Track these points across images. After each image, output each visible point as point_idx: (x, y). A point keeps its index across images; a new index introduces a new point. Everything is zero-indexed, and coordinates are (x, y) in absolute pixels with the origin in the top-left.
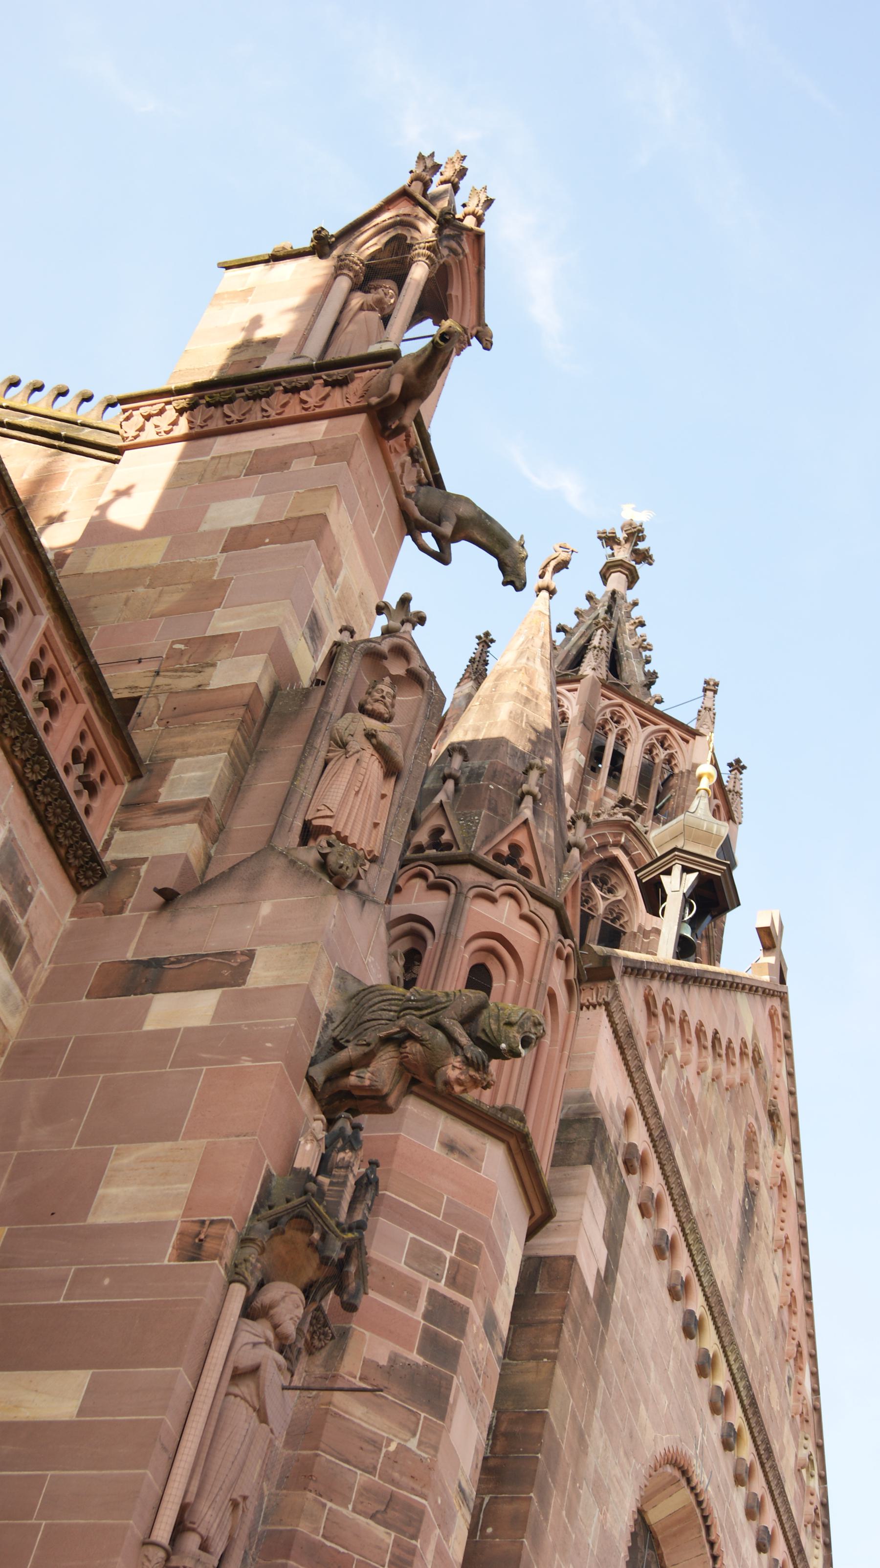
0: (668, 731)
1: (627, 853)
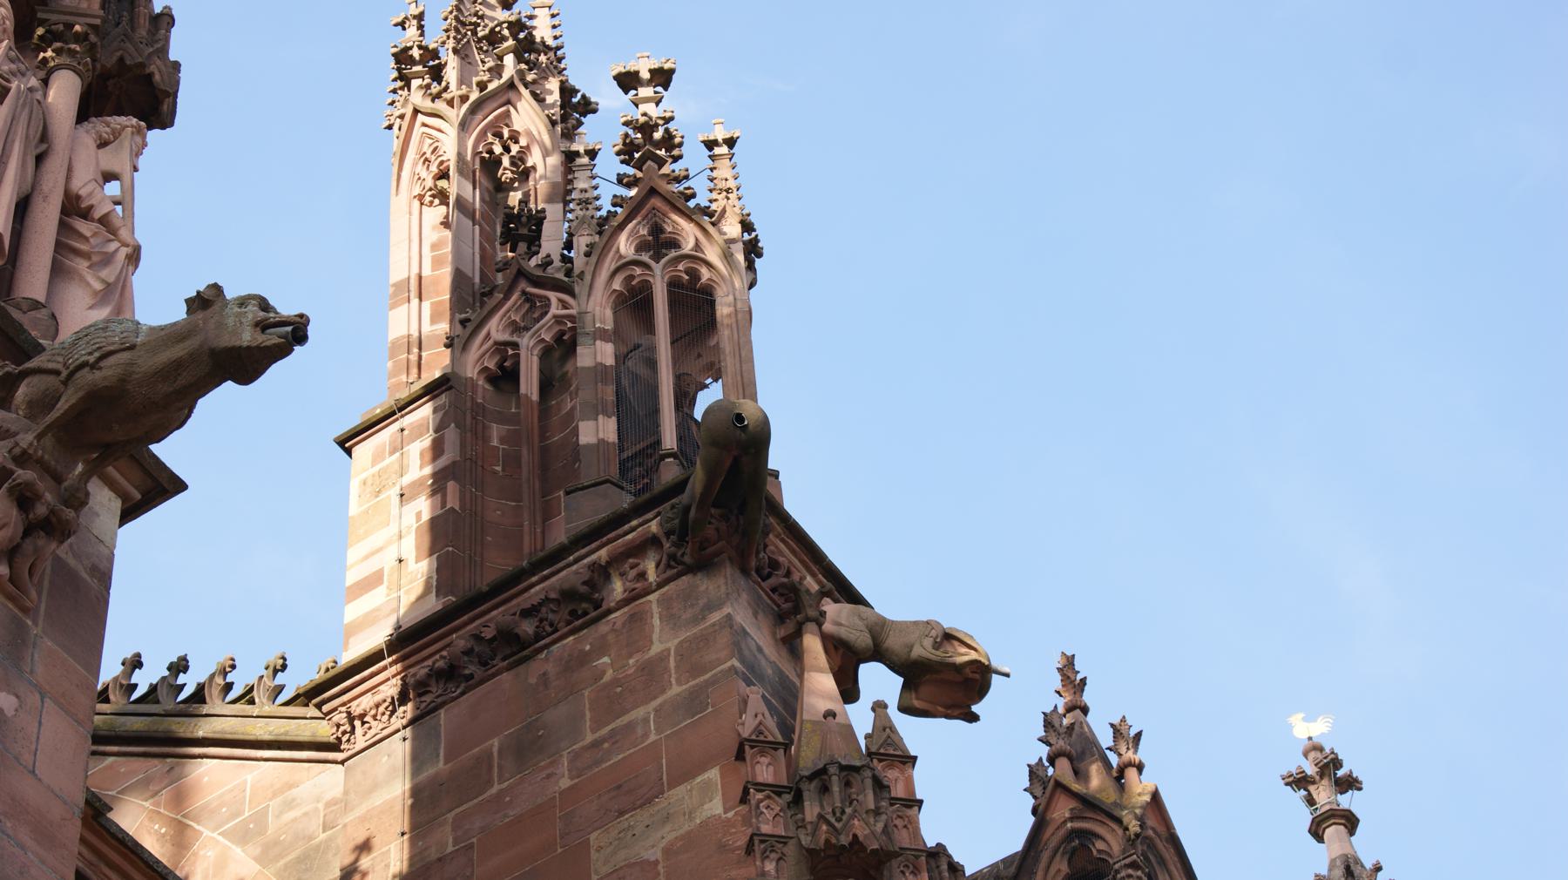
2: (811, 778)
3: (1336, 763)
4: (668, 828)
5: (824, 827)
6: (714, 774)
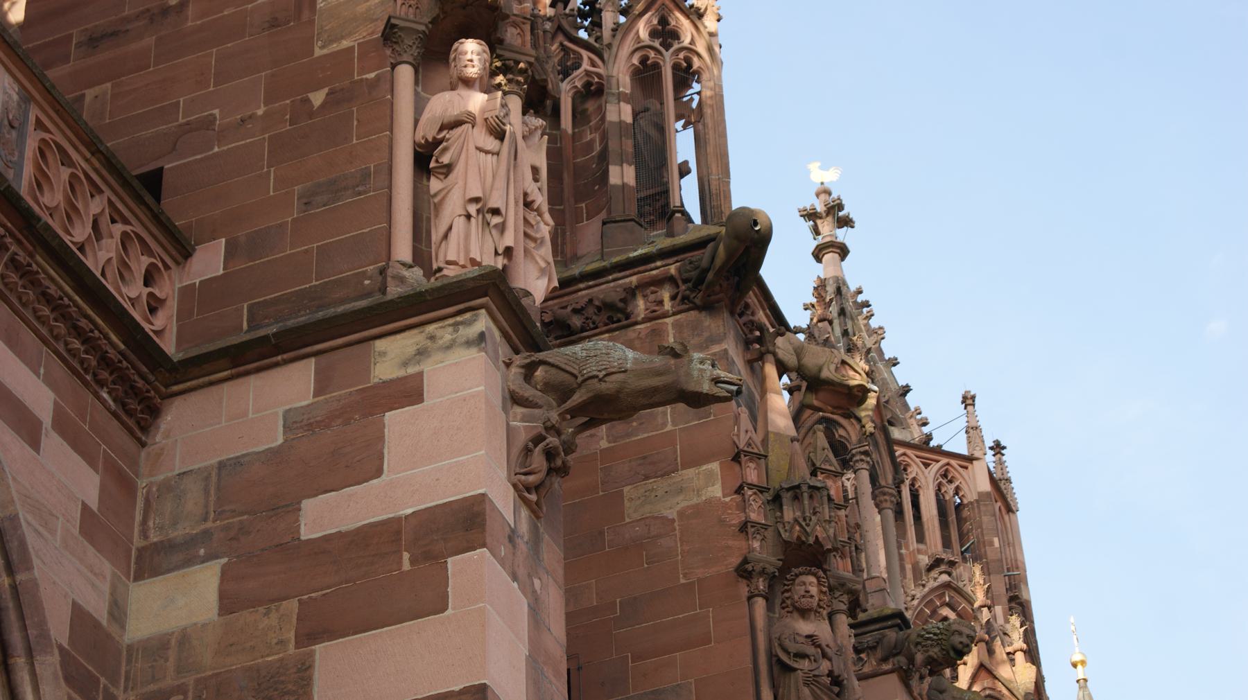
0: (948, 464)
1: (953, 609)
2: (788, 490)
3: (840, 207)
4: (681, 497)
5: (797, 528)
6: (715, 466)
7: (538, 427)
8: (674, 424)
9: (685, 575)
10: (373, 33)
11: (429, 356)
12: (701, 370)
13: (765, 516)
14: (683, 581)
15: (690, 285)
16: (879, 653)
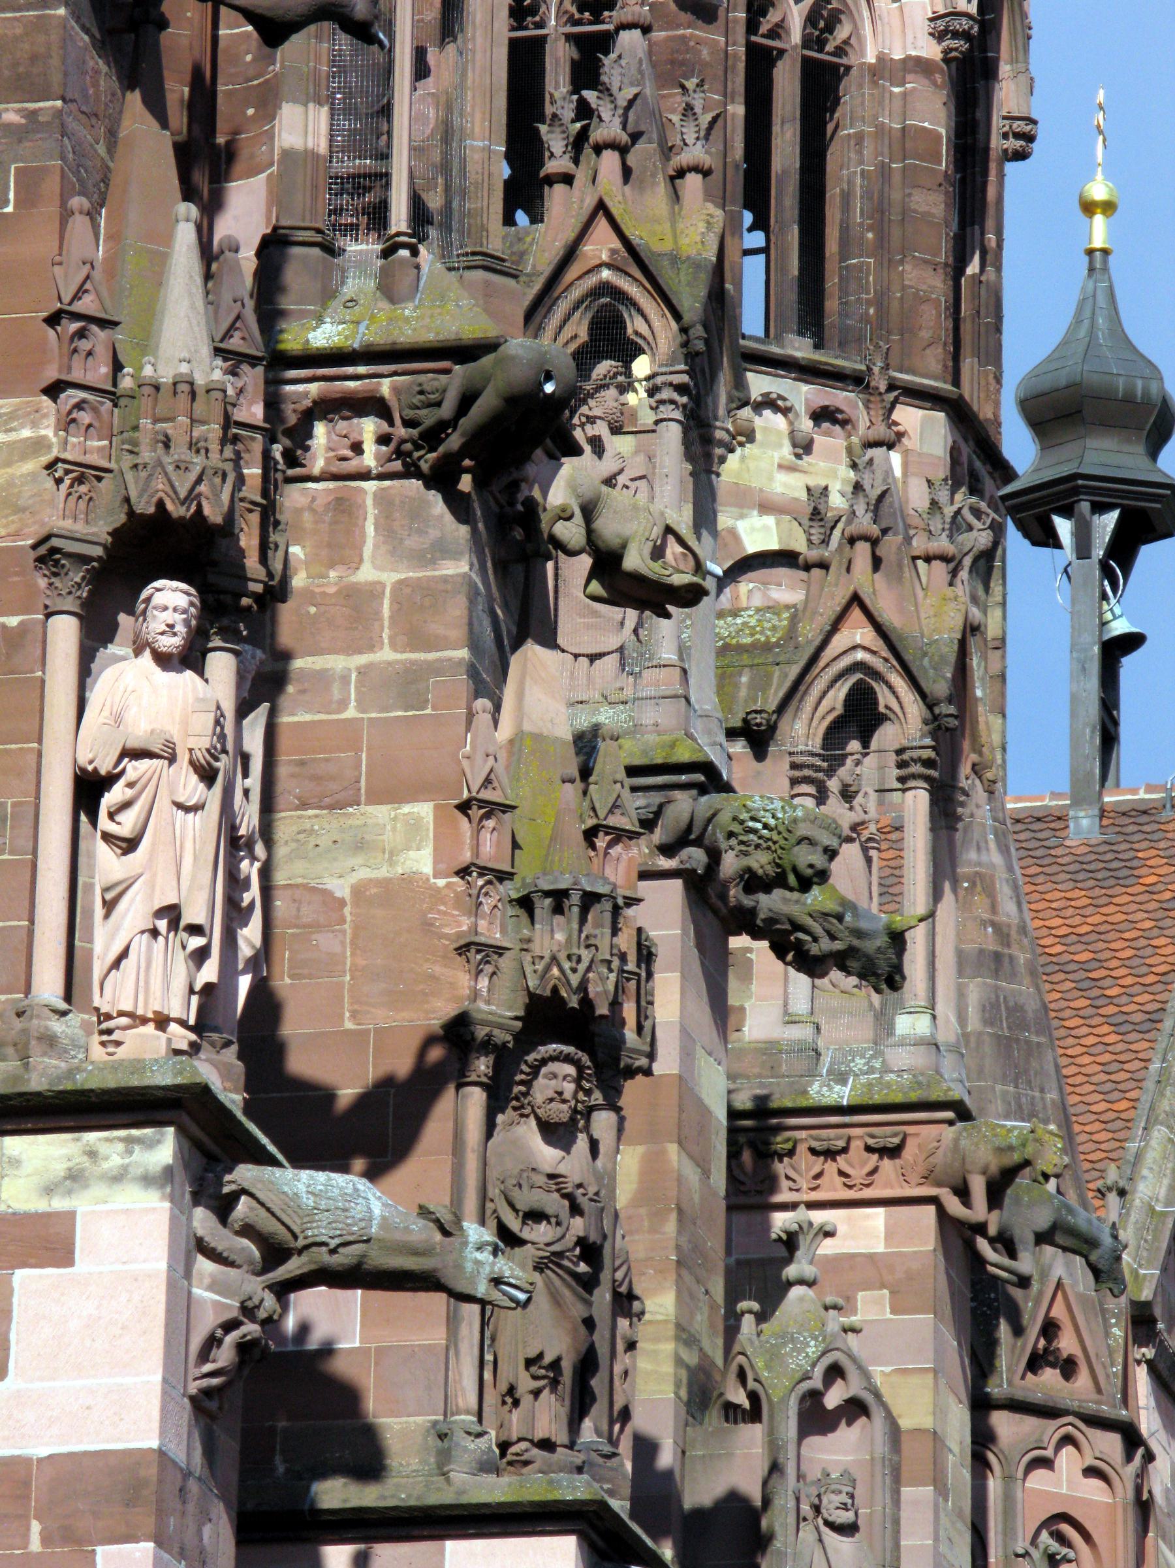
2: (547, 894)
4: (358, 860)
5: (555, 971)
6: (425, 810)
7: (232, 1306)
8: (361, 708)
9: (354, 1015)
10: (16, 535)
11: (86, 1187)
12: (478, 1263)
13: (503, 931)
14: (349, 1025)
15: (415, 432)
16: (658, 836)
